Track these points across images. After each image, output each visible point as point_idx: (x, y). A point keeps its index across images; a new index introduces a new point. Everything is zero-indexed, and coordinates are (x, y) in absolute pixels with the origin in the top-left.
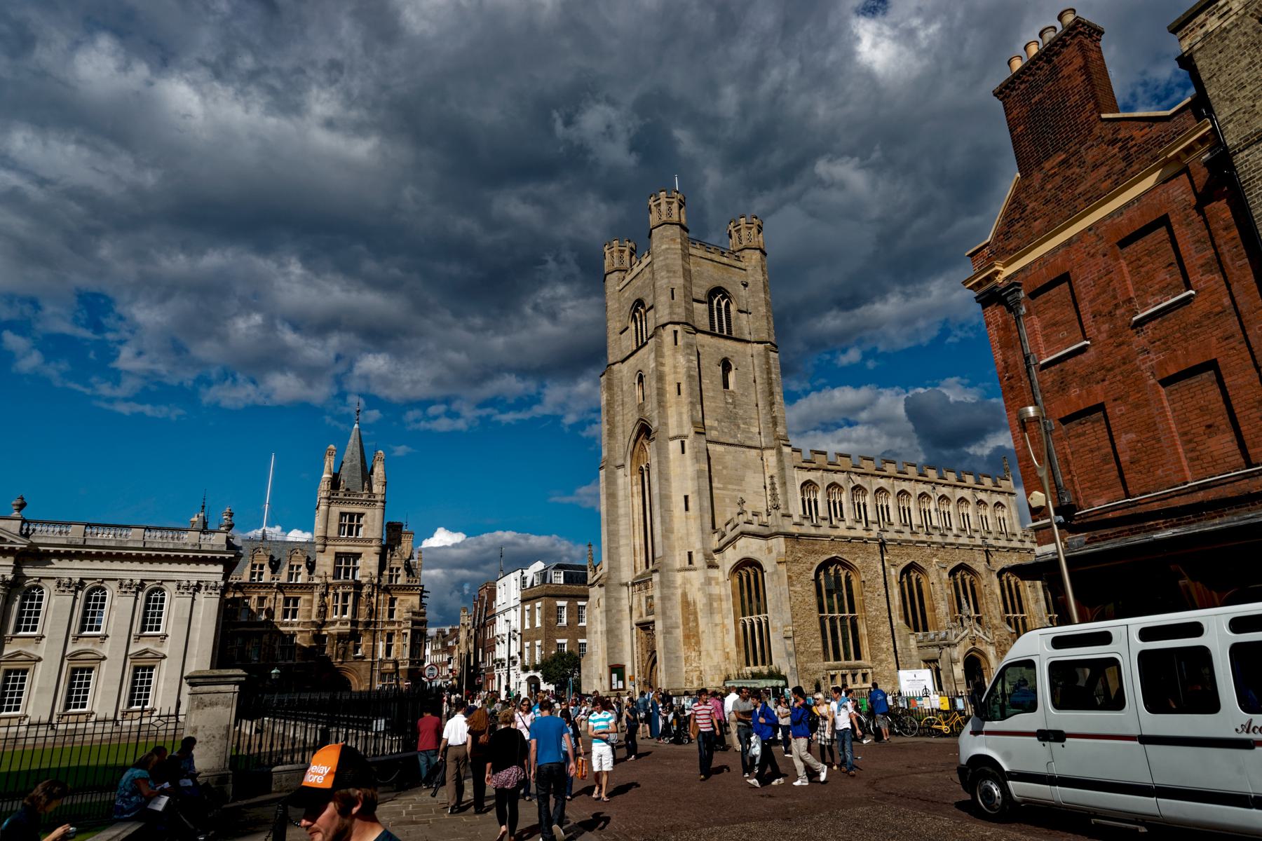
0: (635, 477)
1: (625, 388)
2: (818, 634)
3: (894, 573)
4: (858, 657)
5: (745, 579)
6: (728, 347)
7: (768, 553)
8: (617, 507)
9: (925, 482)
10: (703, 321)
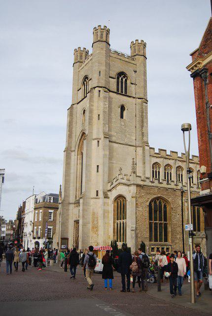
1: (78, 115)
2: (148, 230)
4: (166, 240)
6: (123, 100)
7: (129, 192)
8: (70, 169)
10: (113, 87)
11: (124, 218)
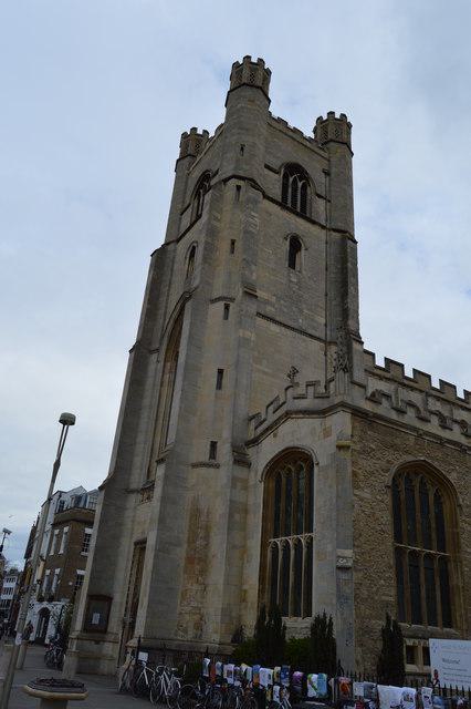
0: (169, 364)
2: (391, 574)
5: (284, 480)
6: (299, 226)
7: (319, 438)
8: (142, 397)
11: (310, 529)
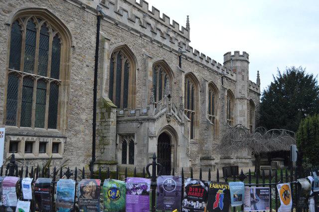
3: (108, 48)
4: (53, 124)
9: (139, 10)
